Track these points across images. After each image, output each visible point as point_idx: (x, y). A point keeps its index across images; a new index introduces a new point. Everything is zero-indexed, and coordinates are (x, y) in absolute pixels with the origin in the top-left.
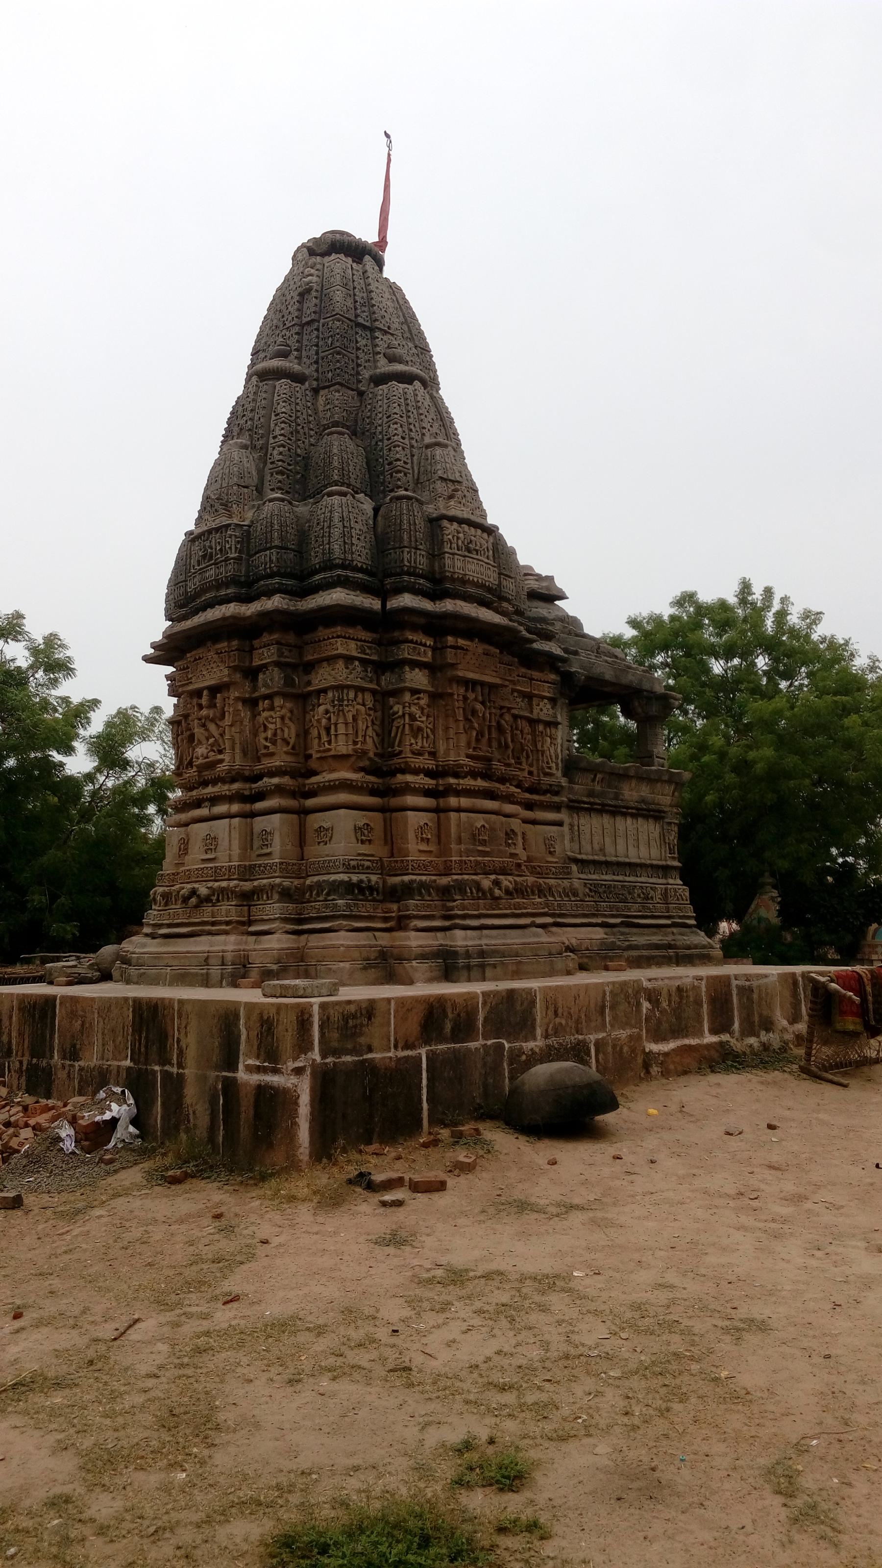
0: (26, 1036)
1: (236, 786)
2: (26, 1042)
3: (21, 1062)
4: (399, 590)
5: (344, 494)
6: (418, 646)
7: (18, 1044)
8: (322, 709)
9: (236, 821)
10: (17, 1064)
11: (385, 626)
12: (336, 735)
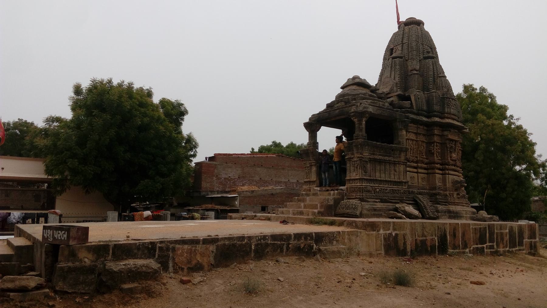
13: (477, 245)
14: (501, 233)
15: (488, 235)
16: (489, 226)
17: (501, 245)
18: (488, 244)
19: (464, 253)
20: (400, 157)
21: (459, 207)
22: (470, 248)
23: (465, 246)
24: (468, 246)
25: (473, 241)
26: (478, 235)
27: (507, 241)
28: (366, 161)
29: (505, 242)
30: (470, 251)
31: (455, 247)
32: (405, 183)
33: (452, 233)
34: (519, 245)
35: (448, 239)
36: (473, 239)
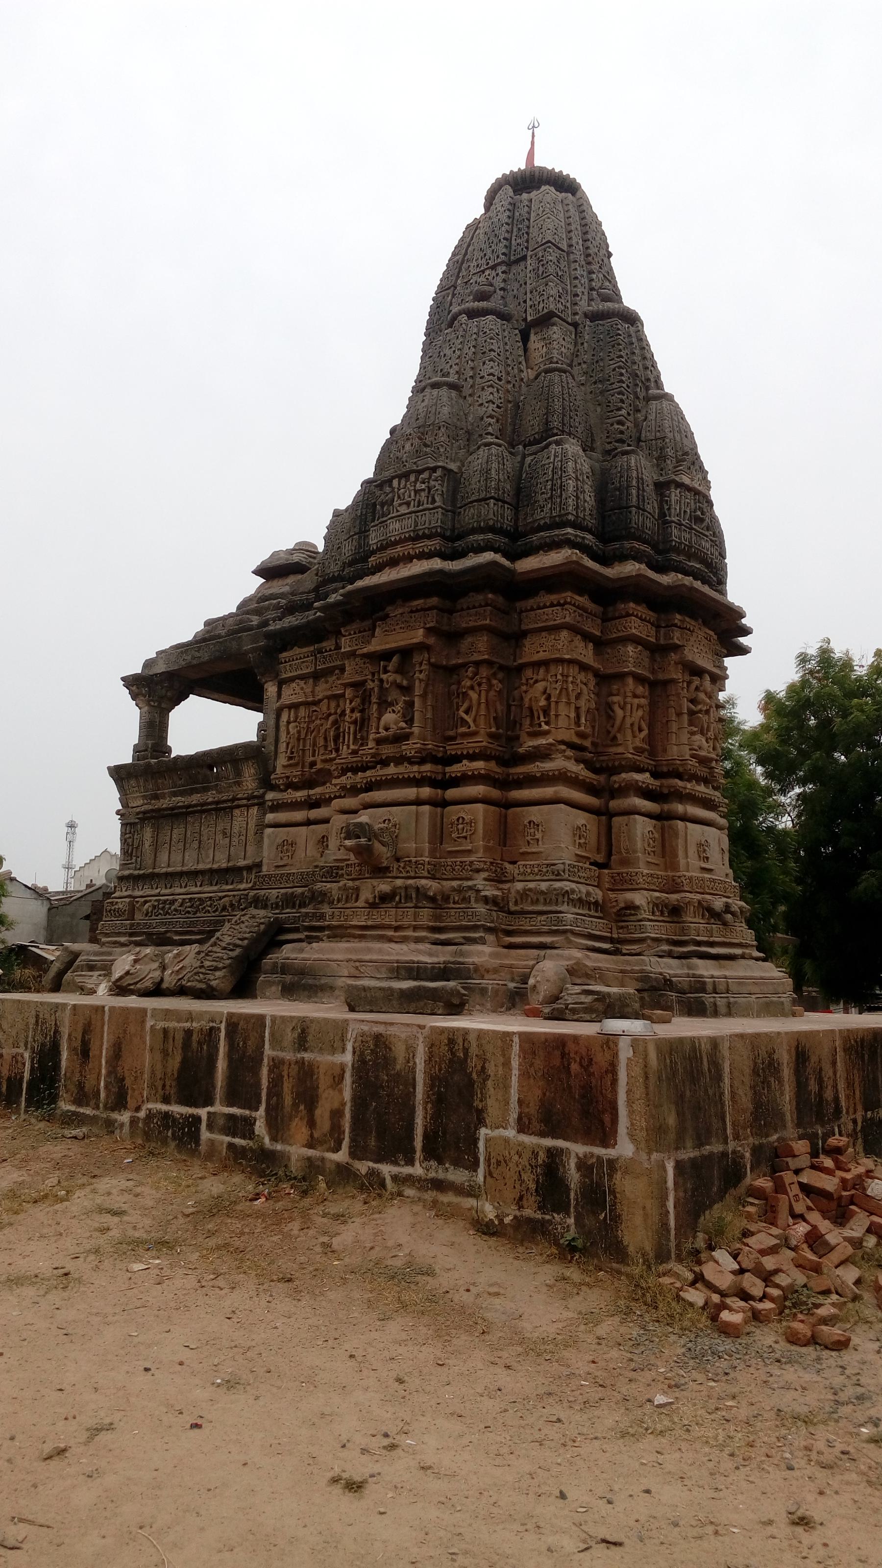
0: (856, 1084)
1: (427, 767)
2: (857, 1093)
3: (855, 1121)
4: (623, 558)
5: (500, 446)
6: (637, 623)
7: (848, 1097)
8: (540, 686)
9: (426, 808)
10: (850, 1126)
11: (607, 596)
12: (557, 716)
13: (166, 1100)
14: (301, 1063)
15: (221, 1065)
16: (234, 1024)
17: (299, 1130)
18: (220, 1108)
19: (110, 1126)
20: (239, 784)
21: (343, 945)
22: (138, 1109)
23: (119, 1102)
24: (131, 1103)
25: (152, 1086)
26: (175, 1062)
27: (336, 1114)
28: (135, 824)
29: (322, 1113)
30: (134, 1121)
31: (82, 1097)
32: (249, 868)
33: (78, 1044)
34: (432, 1152)
35: (64, 1064)
36: (153, 1072)
